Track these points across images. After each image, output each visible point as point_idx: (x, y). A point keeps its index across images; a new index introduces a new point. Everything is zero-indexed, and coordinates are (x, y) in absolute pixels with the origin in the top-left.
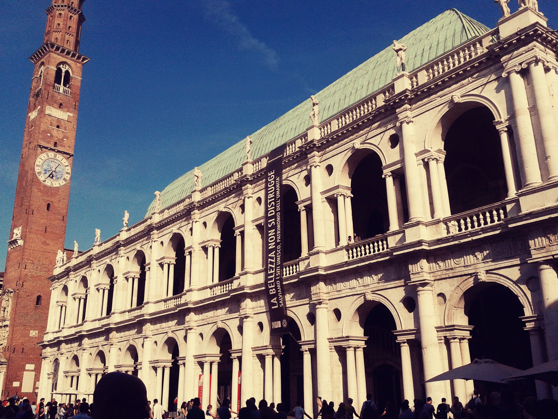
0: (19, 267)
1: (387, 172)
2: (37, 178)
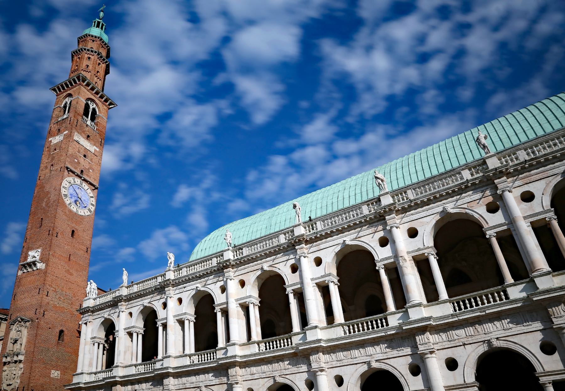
2: (63, 199)
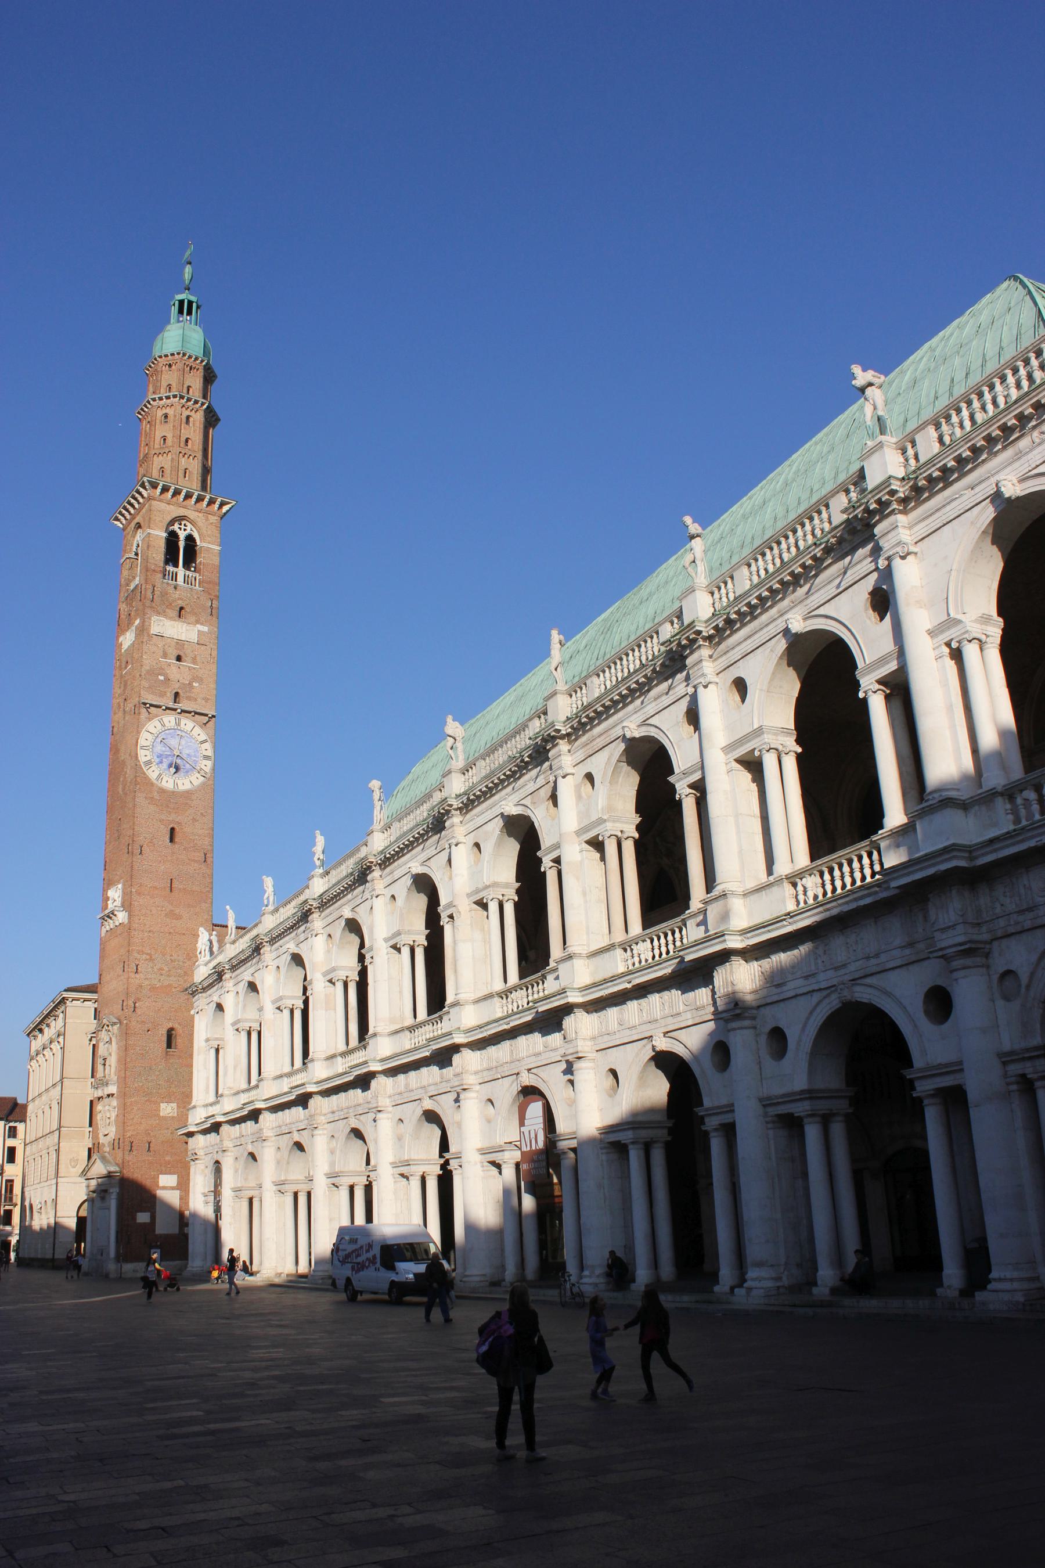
0: (124, 971)
2: (145, 774)
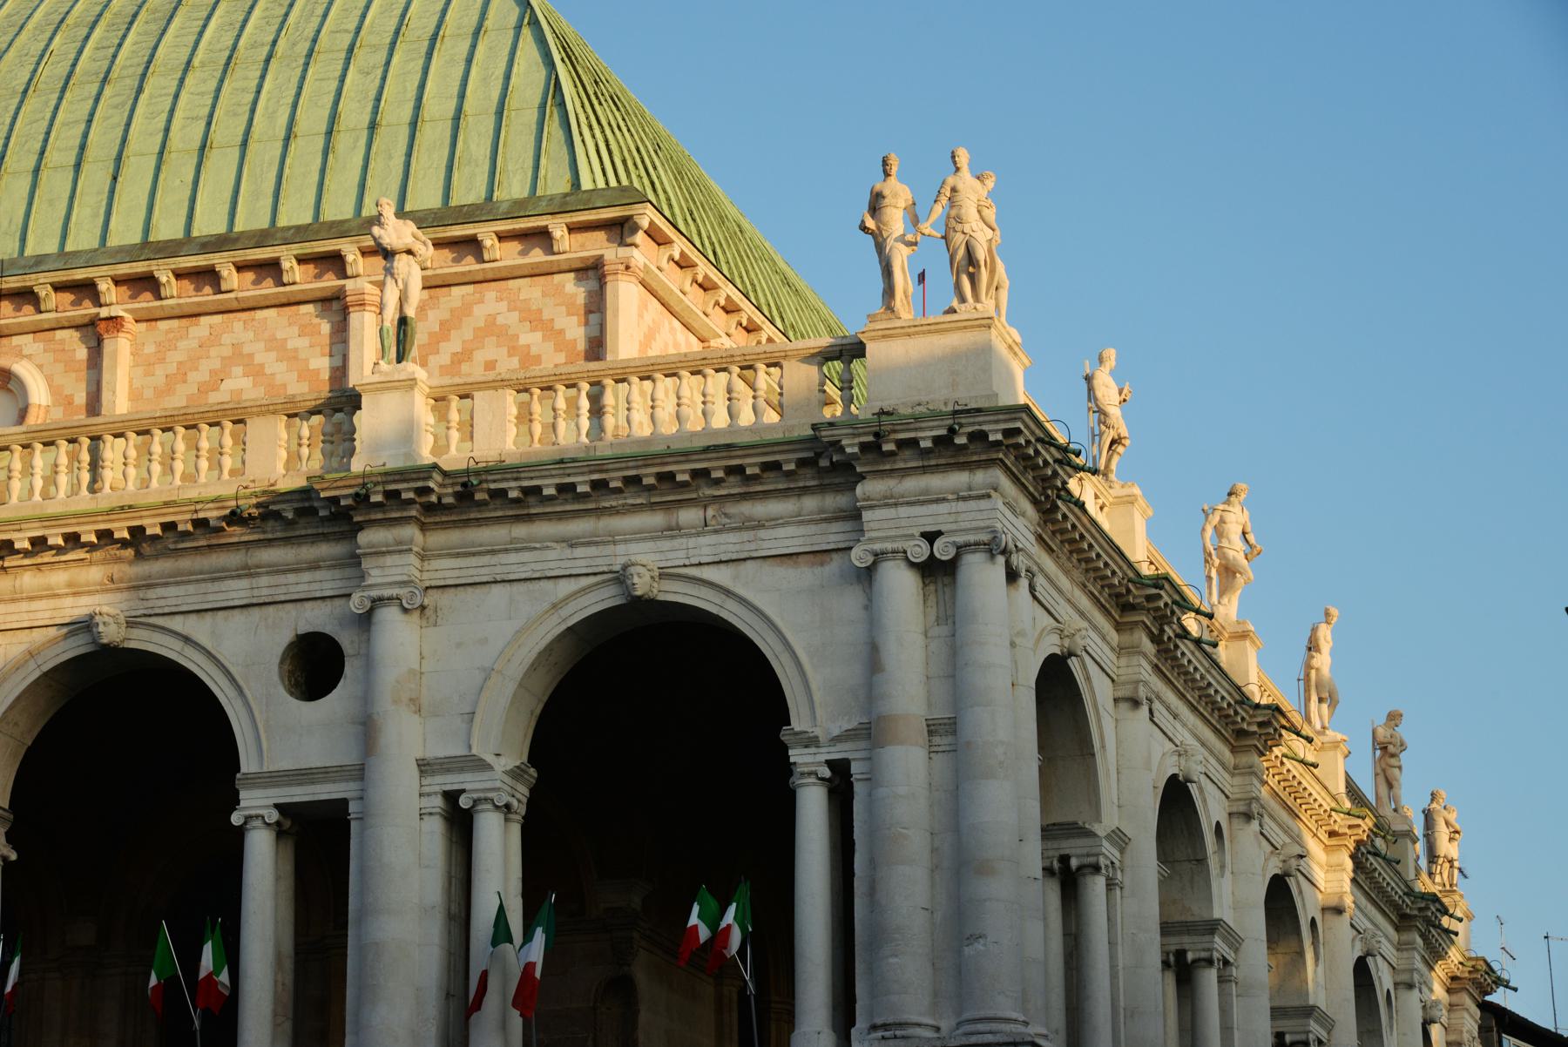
1: (255, 803)
